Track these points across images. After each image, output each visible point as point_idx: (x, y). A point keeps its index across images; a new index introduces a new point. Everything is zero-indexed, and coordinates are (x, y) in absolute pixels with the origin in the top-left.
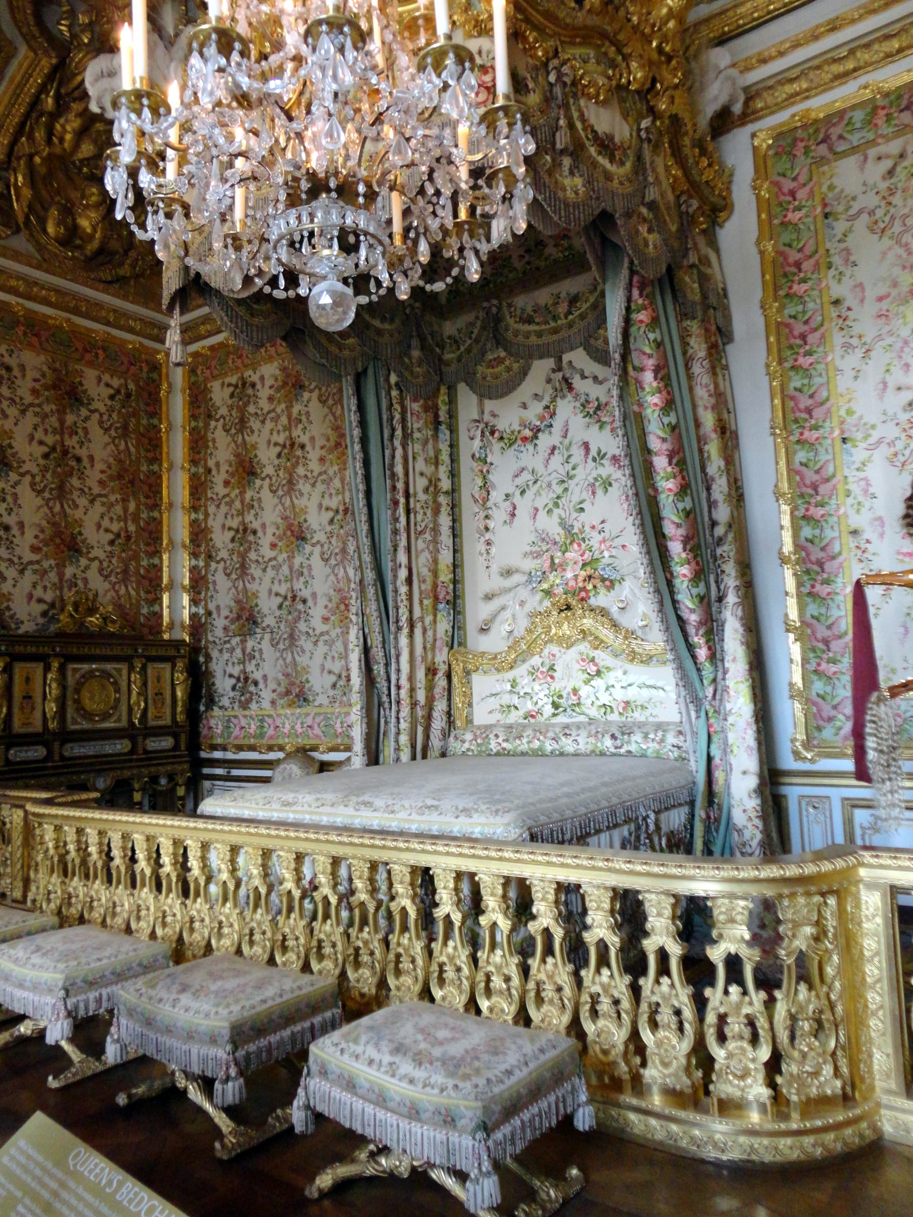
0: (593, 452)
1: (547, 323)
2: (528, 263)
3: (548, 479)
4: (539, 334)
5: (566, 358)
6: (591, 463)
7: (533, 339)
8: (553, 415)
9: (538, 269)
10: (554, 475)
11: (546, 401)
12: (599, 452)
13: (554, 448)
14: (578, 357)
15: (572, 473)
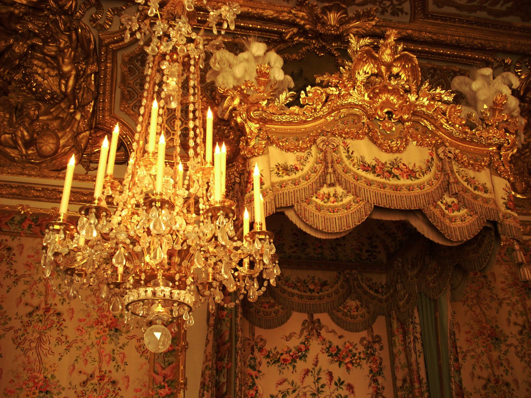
0: (336, 379)
1: (304, 292)
2: (294, 252)
3: (305, 391)
4: (301, 297)
5: (316, 316)
6: (333, 387)
7: (296, 299)
8: (307, 349)
9: (299, 258)
10: (308, 389)
11: (302, 339)
12: (340, 380)
13: (307, 372)
14: (324, 318)
15: (321, 389)
